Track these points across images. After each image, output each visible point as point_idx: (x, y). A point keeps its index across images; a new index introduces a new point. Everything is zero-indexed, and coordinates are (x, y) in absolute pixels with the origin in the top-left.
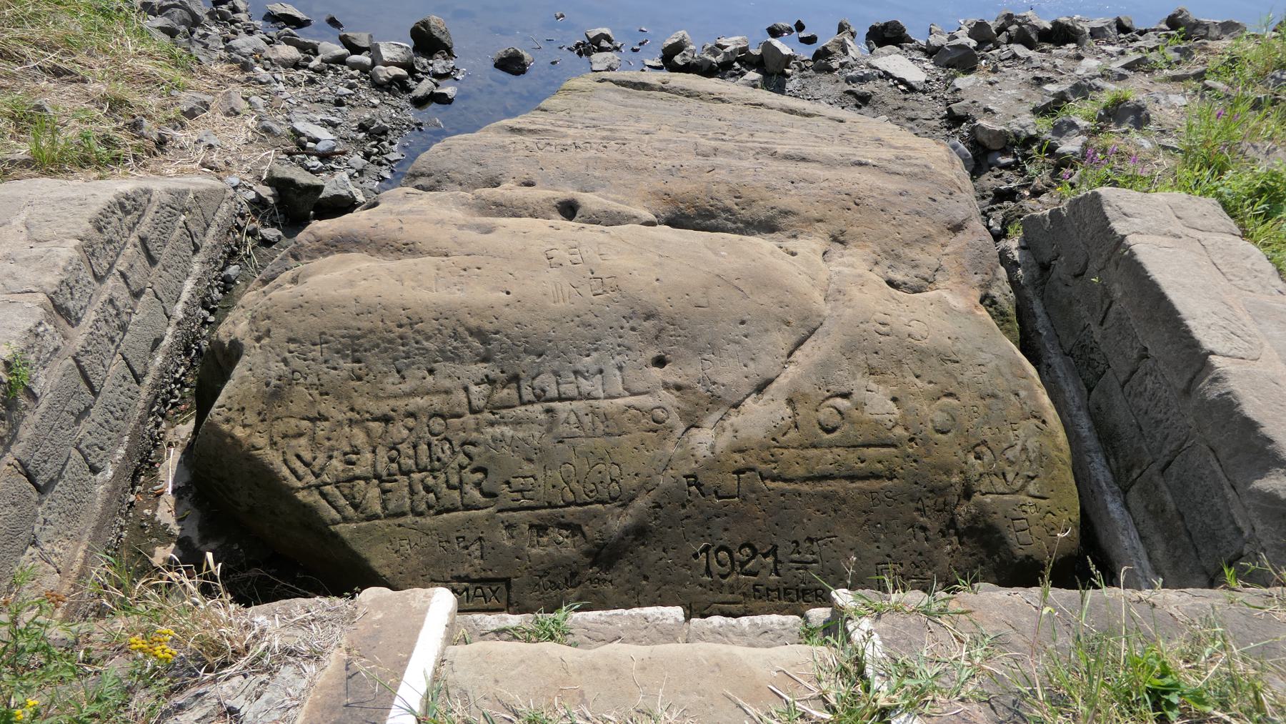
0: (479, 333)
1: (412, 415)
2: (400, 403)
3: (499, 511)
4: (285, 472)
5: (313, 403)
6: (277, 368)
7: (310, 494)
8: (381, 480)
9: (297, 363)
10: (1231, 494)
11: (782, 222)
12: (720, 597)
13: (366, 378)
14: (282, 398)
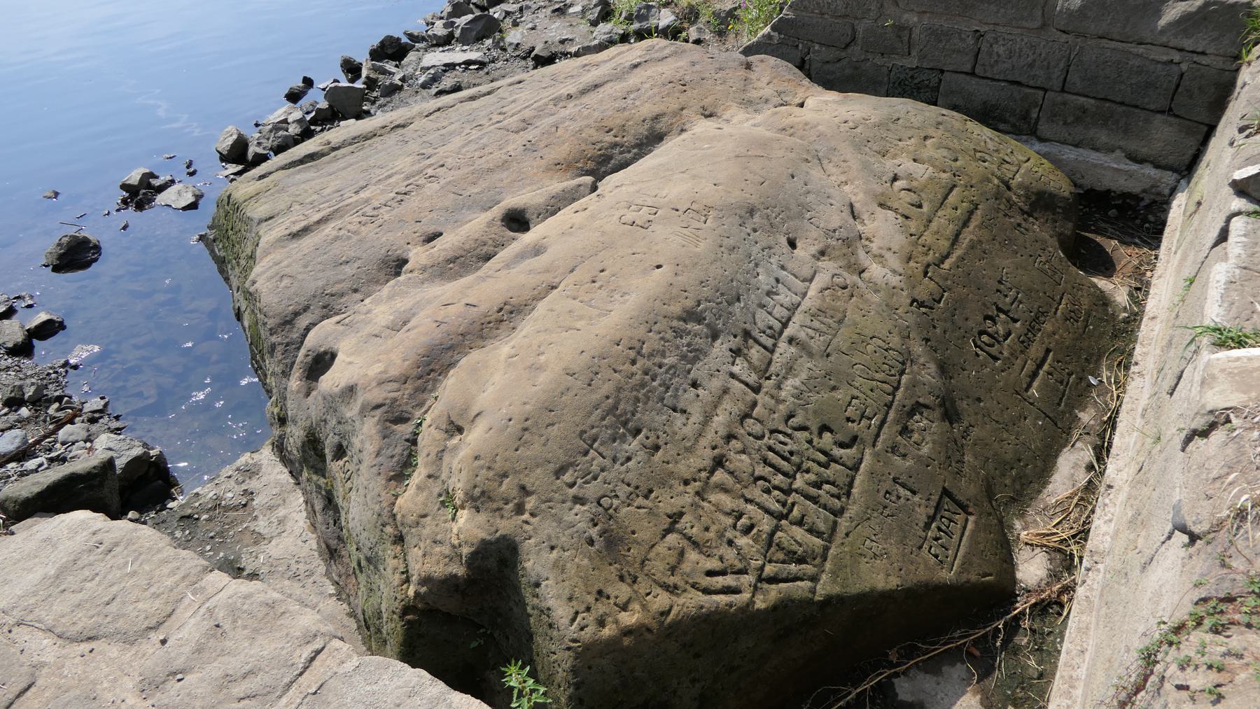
0: (690, 315)
1: (730, 437)
2: (709, 437)
3: (874, 446)
4: (722, 599)
5: (651, 512)
6: (579, 516)
7: (767, 592)
8: (786, 517)
9: (592, 490)
10: (1141, 49)
11: (661, 126)
12: (1017, 367)
13: (661, 442)
14: (621, 539)
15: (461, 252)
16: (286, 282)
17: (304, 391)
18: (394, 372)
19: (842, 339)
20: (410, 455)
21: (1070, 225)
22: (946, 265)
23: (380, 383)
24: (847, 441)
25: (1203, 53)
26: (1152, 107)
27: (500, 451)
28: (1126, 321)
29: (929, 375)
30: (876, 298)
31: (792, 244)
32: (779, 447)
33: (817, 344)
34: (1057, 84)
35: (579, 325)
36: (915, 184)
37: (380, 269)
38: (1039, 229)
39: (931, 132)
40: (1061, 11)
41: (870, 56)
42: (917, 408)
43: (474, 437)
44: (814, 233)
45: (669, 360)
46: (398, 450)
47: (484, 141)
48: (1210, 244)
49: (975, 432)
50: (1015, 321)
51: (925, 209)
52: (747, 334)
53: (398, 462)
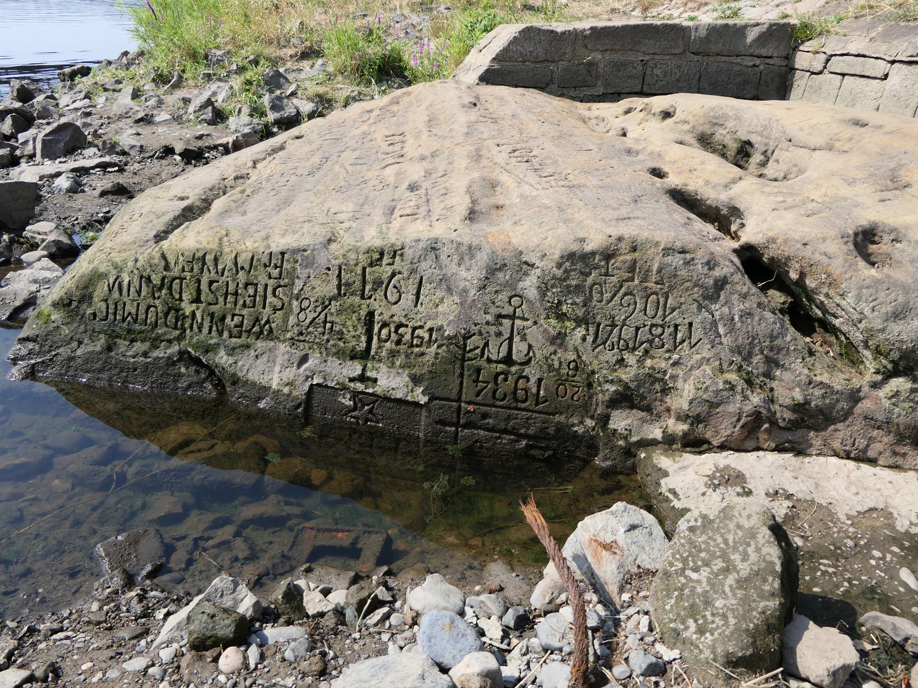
10: (738, 60)
25: (771, 57)
40: (695, 39)
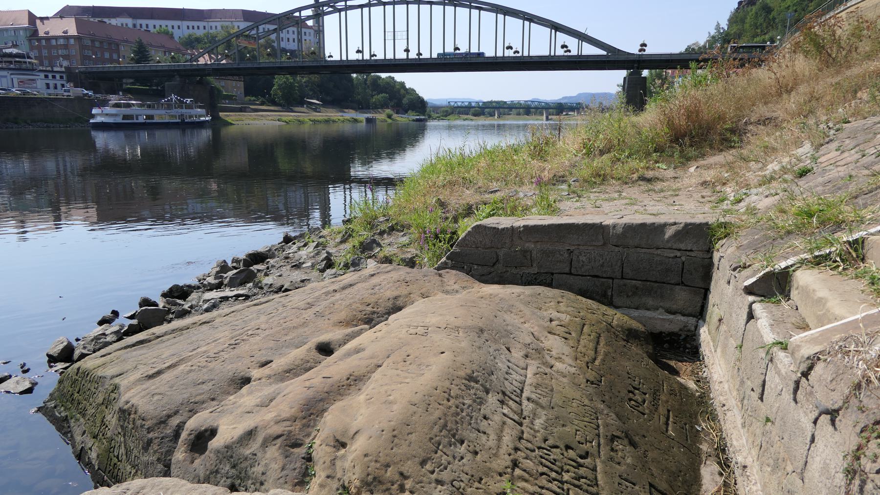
0: (470, 378)
1: (516, 449)
10: (659, 252)
11: (399, 303)
15: (292, 367)
16: (156, 398)
17: (189, 459)
18: (285, 415)
19: (557, 399)
20: (307, 468)
21: (650, 347)
22: (597, 363)
23: (277, 422)
24: (583, 454)
25: (691, 251)
26: (673, 282)
27: (381, 449)
28: (700, 397)
29: (612, 419)
30: (565, 380)
31: (508, 349)
32: (546, 457)
33: (544, 401)
34: (619, 275)
35: (407, 381)
36: (563, 323)
37: (230, 385)
38: (635, 349)
39: (560, 299)
41: (509, 269)
42: (613, 438)
43: (358, 446)
44: (519, 346)
45: (468, 402)
46: (298, 465)
47: (284, 314)
48: (744, 322)
49: (650, 454)
50: (645, 394)
51: (574, 334)
52: (504, 393)
53: (299, 472)
